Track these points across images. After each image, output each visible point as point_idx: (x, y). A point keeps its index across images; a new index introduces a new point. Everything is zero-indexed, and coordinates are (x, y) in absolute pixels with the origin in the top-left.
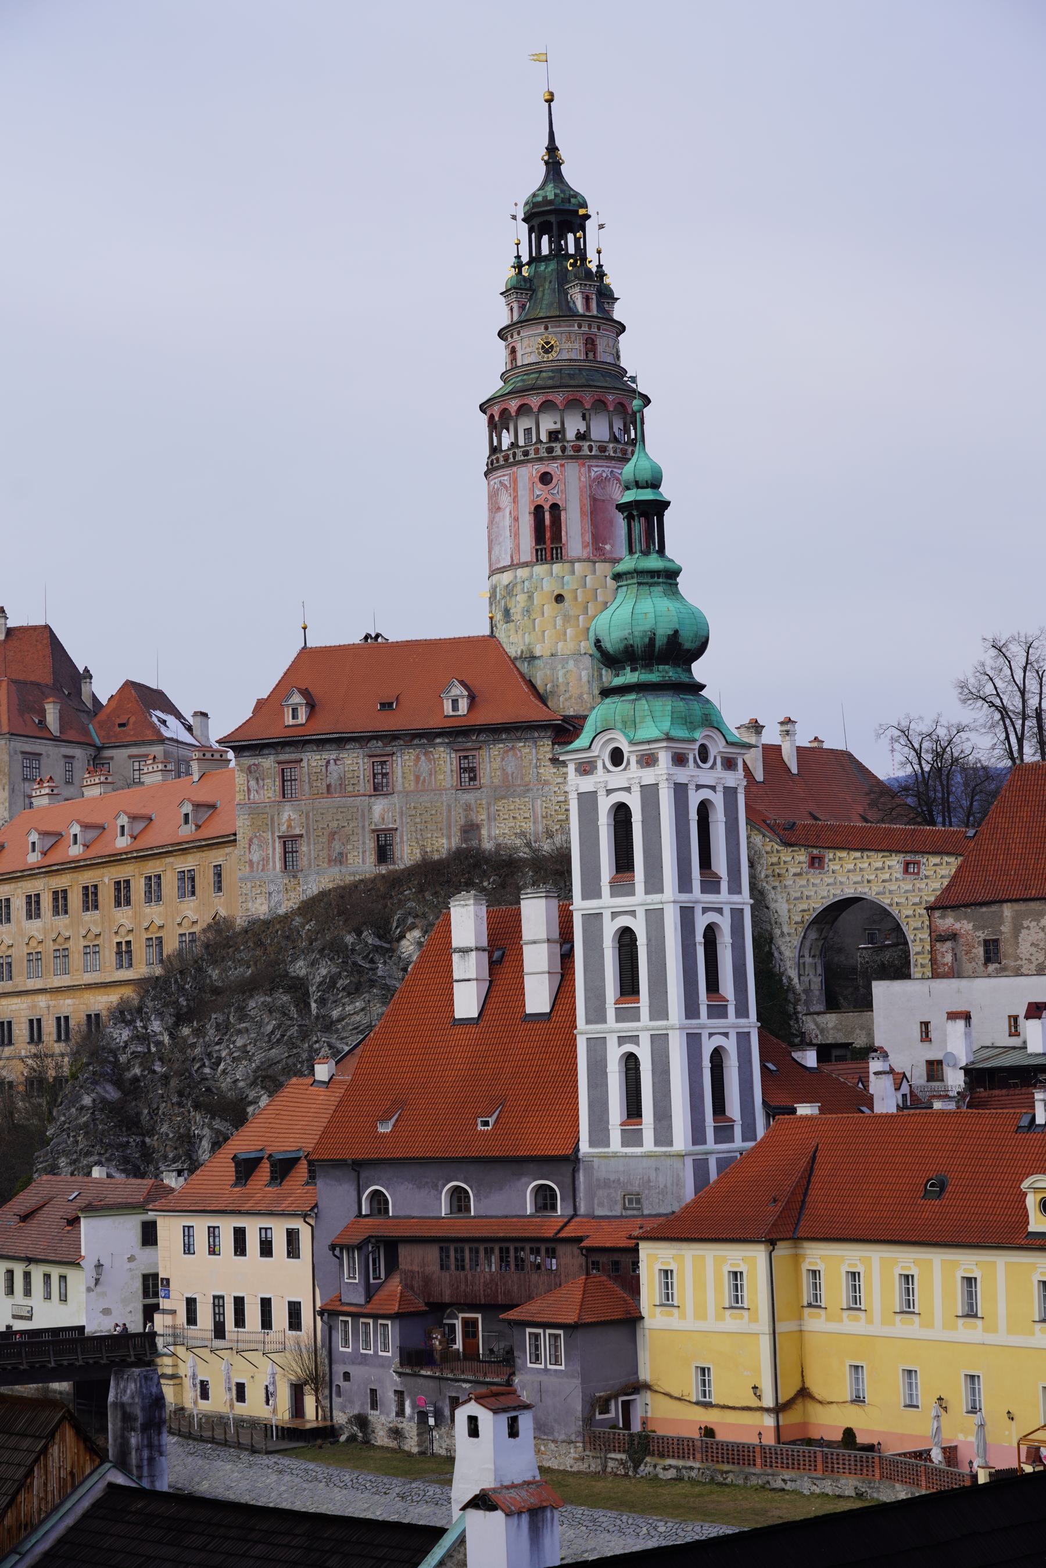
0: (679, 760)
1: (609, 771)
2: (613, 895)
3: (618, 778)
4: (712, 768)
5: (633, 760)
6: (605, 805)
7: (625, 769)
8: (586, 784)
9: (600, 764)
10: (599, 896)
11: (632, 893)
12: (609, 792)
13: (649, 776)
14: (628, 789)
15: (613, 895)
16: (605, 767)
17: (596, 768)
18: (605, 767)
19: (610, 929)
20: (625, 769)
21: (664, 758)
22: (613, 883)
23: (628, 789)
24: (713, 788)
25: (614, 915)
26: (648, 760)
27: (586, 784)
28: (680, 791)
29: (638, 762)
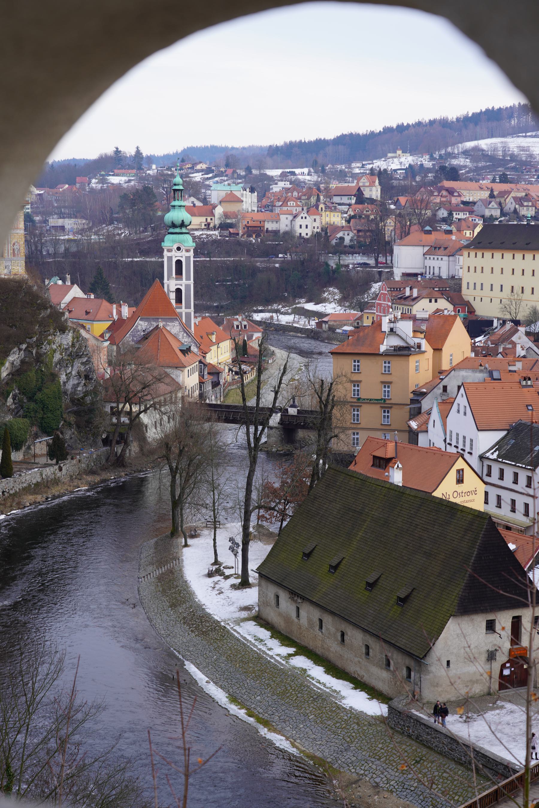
3: (179, 253)
6: (174, 260)
8: (169, 254)
13: (187, 254)
26: (188, 251)
27: (169, 254)
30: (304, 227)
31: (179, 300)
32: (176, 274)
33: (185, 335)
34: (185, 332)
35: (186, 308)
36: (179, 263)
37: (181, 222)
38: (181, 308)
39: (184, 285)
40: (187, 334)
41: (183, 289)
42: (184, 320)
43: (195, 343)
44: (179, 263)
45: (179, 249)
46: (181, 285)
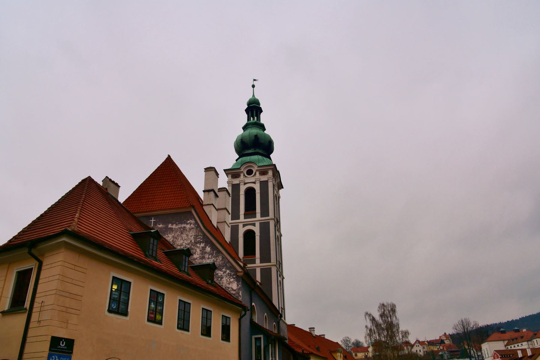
0: (274, 175)
1: (246, 177)
2: (245, 218)
3: (250, 179)
5: (258, 173)
6: (243, 189)
8: (236, 181)
10: (238, 218)
12: (245, 184)
13: (264, 178)
14: (254, 183)
15: (245, 218)
16: (244, 175)
18: (244, 175)
19: (242, 231)
21: (270, 173)
22: (245, 214)
27: (236, 181)
28: (274, 186)
30: (418, 351)
31: (249, 250)
33: (208, 249)
34: (208, 242)
36: (250, 192)
37: (253, 138)
38: (255, 263)
39: (258, 224)
40: (213, 247)
41: (257, 229)
43: (232, 268)
44: (250, 192)
45: (250, 172)
46: (254, 225)
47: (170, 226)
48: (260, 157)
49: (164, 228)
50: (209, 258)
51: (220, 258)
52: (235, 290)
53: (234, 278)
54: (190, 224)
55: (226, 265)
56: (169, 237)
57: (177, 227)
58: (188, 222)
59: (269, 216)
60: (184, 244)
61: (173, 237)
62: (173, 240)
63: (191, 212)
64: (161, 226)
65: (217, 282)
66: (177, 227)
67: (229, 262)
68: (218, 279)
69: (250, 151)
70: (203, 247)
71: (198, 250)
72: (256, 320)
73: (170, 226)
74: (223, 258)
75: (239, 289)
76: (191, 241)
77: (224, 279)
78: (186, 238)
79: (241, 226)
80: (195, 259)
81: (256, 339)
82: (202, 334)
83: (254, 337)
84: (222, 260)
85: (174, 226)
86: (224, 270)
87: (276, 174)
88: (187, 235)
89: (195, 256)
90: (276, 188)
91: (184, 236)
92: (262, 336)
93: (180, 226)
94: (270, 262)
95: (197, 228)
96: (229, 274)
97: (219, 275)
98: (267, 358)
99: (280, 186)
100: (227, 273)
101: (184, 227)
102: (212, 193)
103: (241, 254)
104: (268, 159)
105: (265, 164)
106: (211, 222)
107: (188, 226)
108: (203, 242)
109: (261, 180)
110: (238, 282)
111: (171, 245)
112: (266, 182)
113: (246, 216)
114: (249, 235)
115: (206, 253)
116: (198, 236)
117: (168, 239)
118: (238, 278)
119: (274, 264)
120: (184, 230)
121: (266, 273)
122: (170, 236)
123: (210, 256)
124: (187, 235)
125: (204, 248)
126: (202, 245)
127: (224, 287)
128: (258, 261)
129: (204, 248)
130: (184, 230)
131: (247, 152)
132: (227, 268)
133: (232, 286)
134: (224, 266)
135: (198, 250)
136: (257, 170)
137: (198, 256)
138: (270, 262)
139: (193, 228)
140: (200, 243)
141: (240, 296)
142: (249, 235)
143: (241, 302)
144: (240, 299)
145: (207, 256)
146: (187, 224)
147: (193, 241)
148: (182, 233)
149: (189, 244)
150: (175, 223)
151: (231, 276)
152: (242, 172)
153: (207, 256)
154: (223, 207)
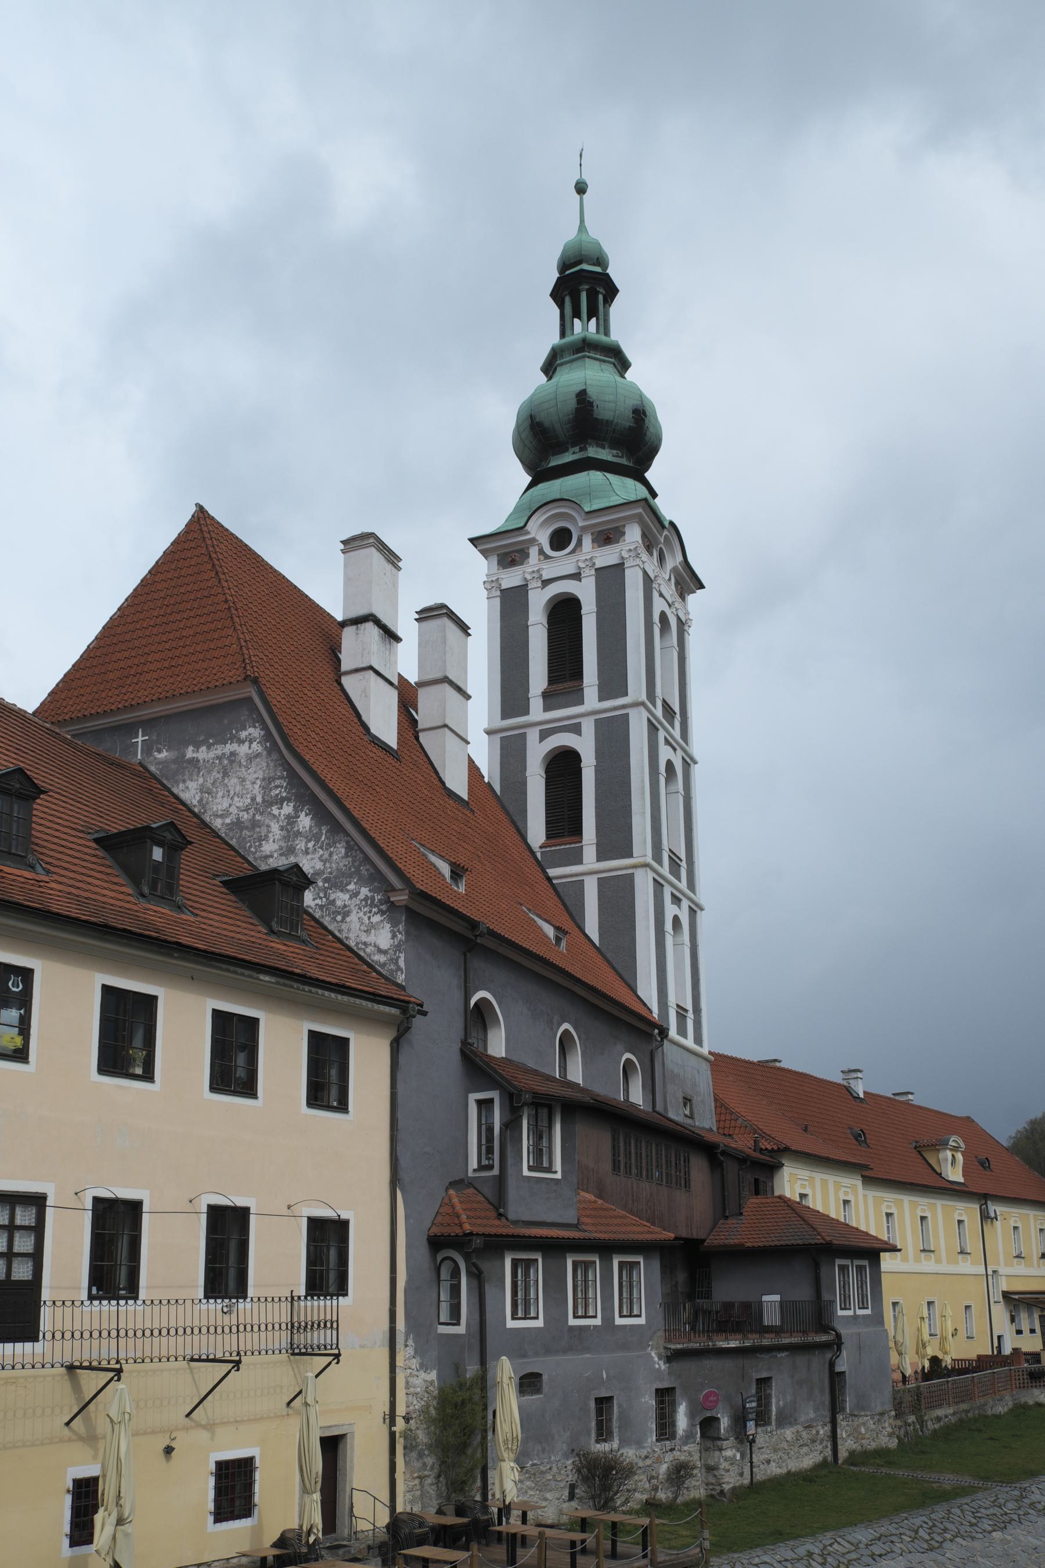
3: (563, 563)
4: (670, 579)
5: (587, 541)
6: (538, 601)
7: (573, 551)
9: (534, 552)
11: (581, 702)
12: (546, 583)
13: (607, 557)
14: (577, 576)
15: (547, 709)
16: (541, 552)
17: (527, 556)
18: (541, 552)
19: (537, 753)
20: (573, 551)
21: (633, 534)
22: (545, 695)
23: (577, 576)
24: (670, 606)
25: (544, 735)
26: (607, 537)
27: (511, 578)
28: (648, 581)
29: (593, 541)
32: (552, 679)
33: (305, 821)
34: (304, 798)
35: (602, 855)
36: (564, 614)
39: (588, 727)
40: (321, 815)
42: (592, 927)
43: (376, 879)
44: (564, 614)
45: (560, 539)
46: (576, 729)
47: (190, 753)
48: (595, 477)
49: (175, 761)
50: (306, 852)
51: (341, 849)
52: (384, 952)
53: (382, 913)
54: (251, 742)
55: (358, 871)
56: (190, 792)
57: (212, 755)
58: (243, 734)
59: (627, 695)
60: (233, 810)
61: (203, 790)
62: (200, 801)
63: (250, 699)
64: (163, 755)
65: (331, 927)
66: (212, 755)
67: (367, 859)
68: (334, 919)
69: (568, 458)
70: (288, 817)
71: (275, 827)
72: (497, 1045)
73: (190, 753)
74: (349, 848)
75: (397, 948)
76: (253, 799)
77: (353, 918)
78: (238, 788)
79: (533, 735)
80: (267, 857)
81: (480, 1103)
82: (213, 1089)
83: (473, 1097)
84: (346, 856)
85: (203, 754)
86: (351, 887)
87: (662, 534)
88: (243, 780)
89: (268, 847)
90: (670, 591)
91: (233, 782)
92: (494, 1095)
93: (219, 752)
94: (630, 855)
95: (269, 753)
96: (366, 899)
97: (339, 903)
98: (510, 1161)
99: (688, 581)
100: (362, 896)
101: (233, 754)
102: (370, 627)
103: (536, 831)
104: (630, 482)
105: (615, 500)
106: (366, 728)
107: (243, 750)
108: (289, 800)
109: (600, 563)
110: (394, 924)
111: (196, 816)
112: (618, 569)
113: (550, 698)
114: (563, 767)
115: (298, 833)
116: (274, 779)
117: (185, 796)
118: (391, 909)
119: (641, 860)
120: (231, 762)
121: (618, 896)
122: (193, 785)
123: (310, 845)
124: (243, 780)
125: (291, 820)
126: (288, 809)
127: (352, 944)
128: (589, 852)
129: (291, 820)
130: (231, 762)
131: (556, 461)
132: (362, 882)
133: (373, 934)
134: (351, 876)
135: (275, 827)
136: (584, 529)
137: (276, 847)
138: (630, 855)
139: (258, 755)
140: (280, 802)
141: (399, 969)
142: (563, 767)
143: (402, 987)
144: (401, 978)
145: (300, 844)
146: (241, 742)
147: (259, 799)
148: (226, 774)
149: (247, 810)
150: (204, 742)
151: (372, 905)
152: (533, 541)
153: (300, 844)
154: (438, 675)
